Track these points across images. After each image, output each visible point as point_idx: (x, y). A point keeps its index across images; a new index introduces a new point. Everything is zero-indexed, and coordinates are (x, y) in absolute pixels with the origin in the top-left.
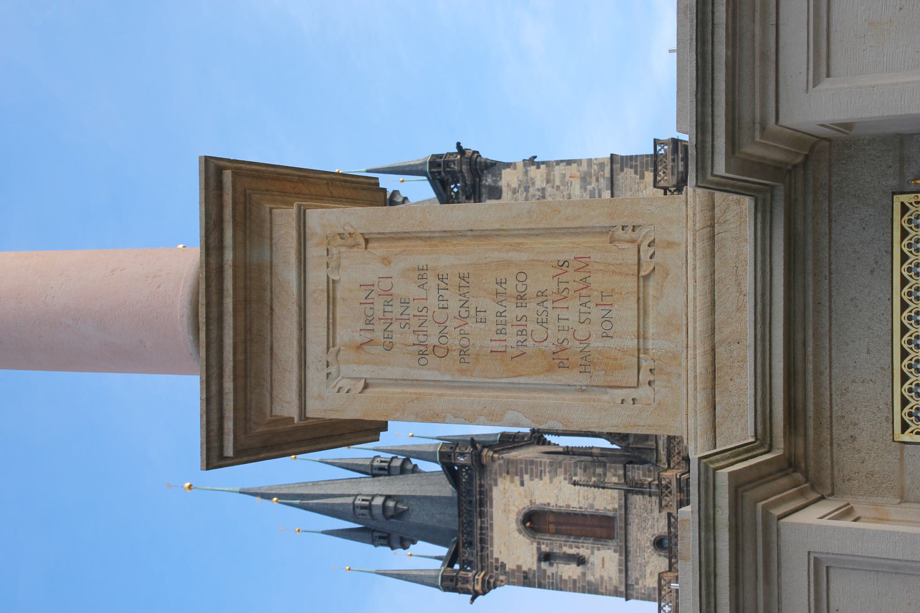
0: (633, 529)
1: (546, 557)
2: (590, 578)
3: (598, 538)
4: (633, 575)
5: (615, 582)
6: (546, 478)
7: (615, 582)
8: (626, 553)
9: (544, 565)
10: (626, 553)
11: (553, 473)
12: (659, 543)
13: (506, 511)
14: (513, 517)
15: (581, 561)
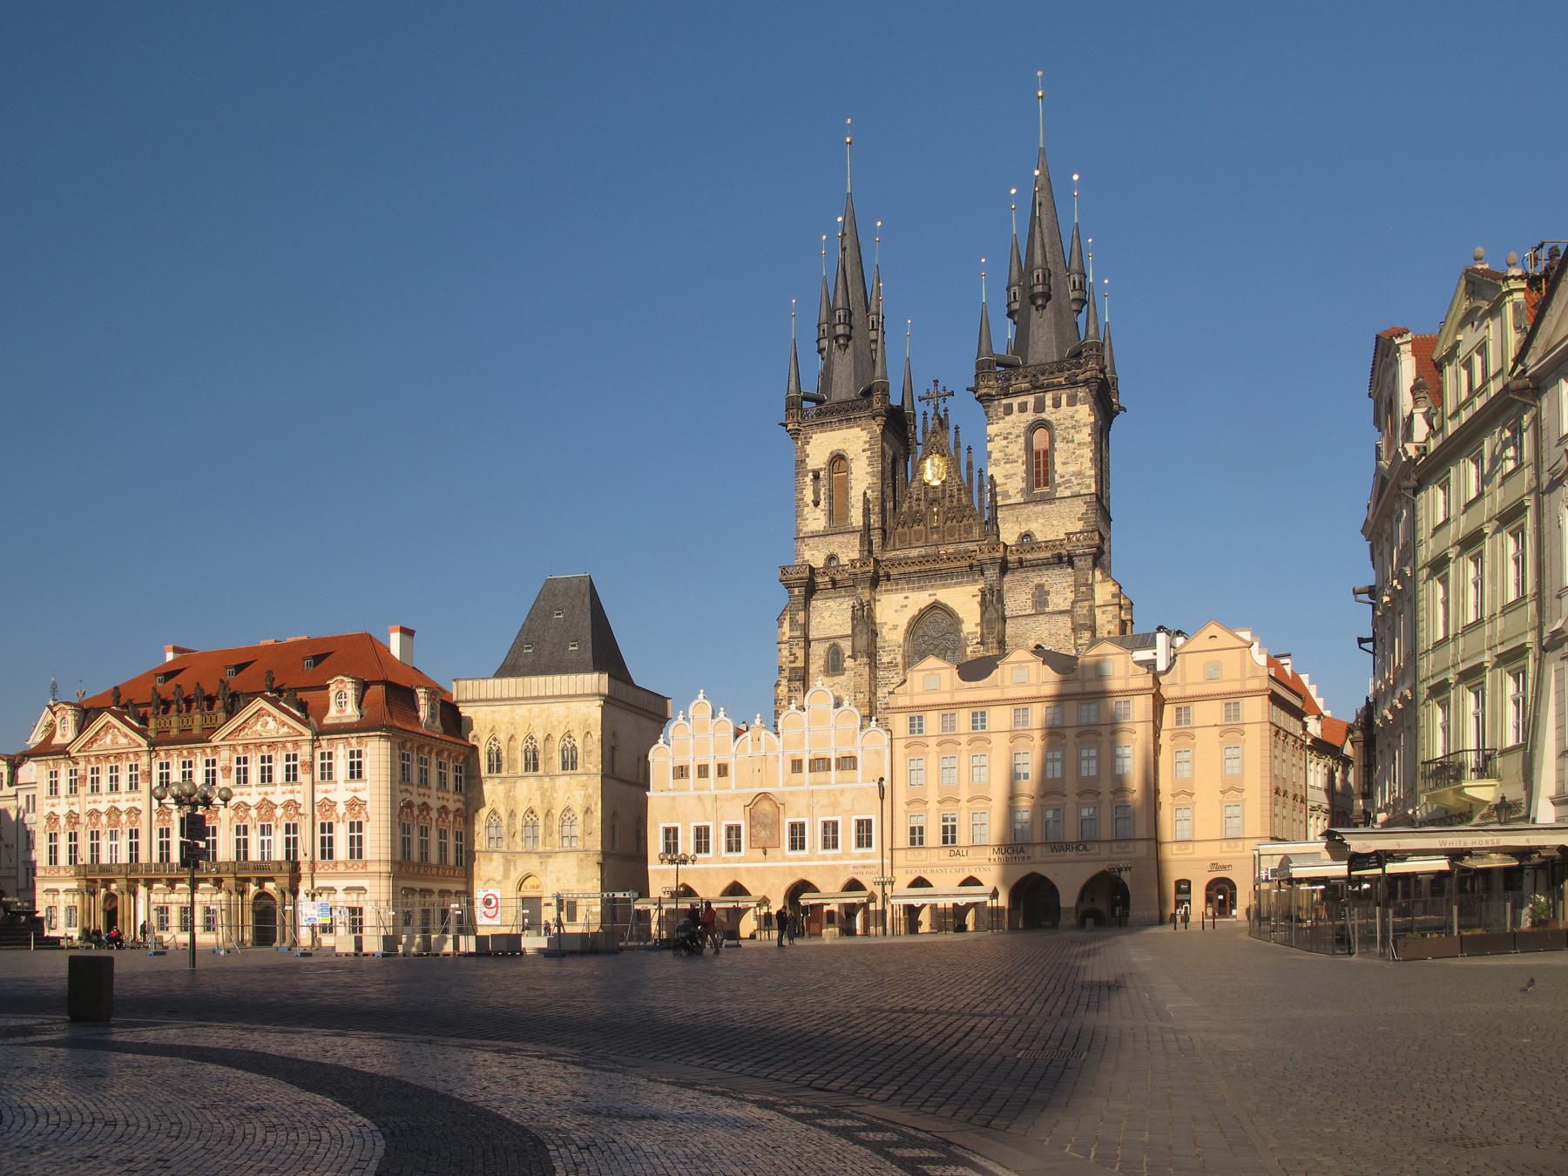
0: (840, 538)
1: (816, 477)
2: (806, 510)
3: (831, 512)
4: (810, 541)
5: (805, 529)
6: (869, 469)
7: (805, 529)
8: (824, 534)
9: (811, 476)
10: (824, 534)
11: (872, 475)
12: (831, 558)
13: (845, 440)
14: (841, 446)
15: (816, 504)
